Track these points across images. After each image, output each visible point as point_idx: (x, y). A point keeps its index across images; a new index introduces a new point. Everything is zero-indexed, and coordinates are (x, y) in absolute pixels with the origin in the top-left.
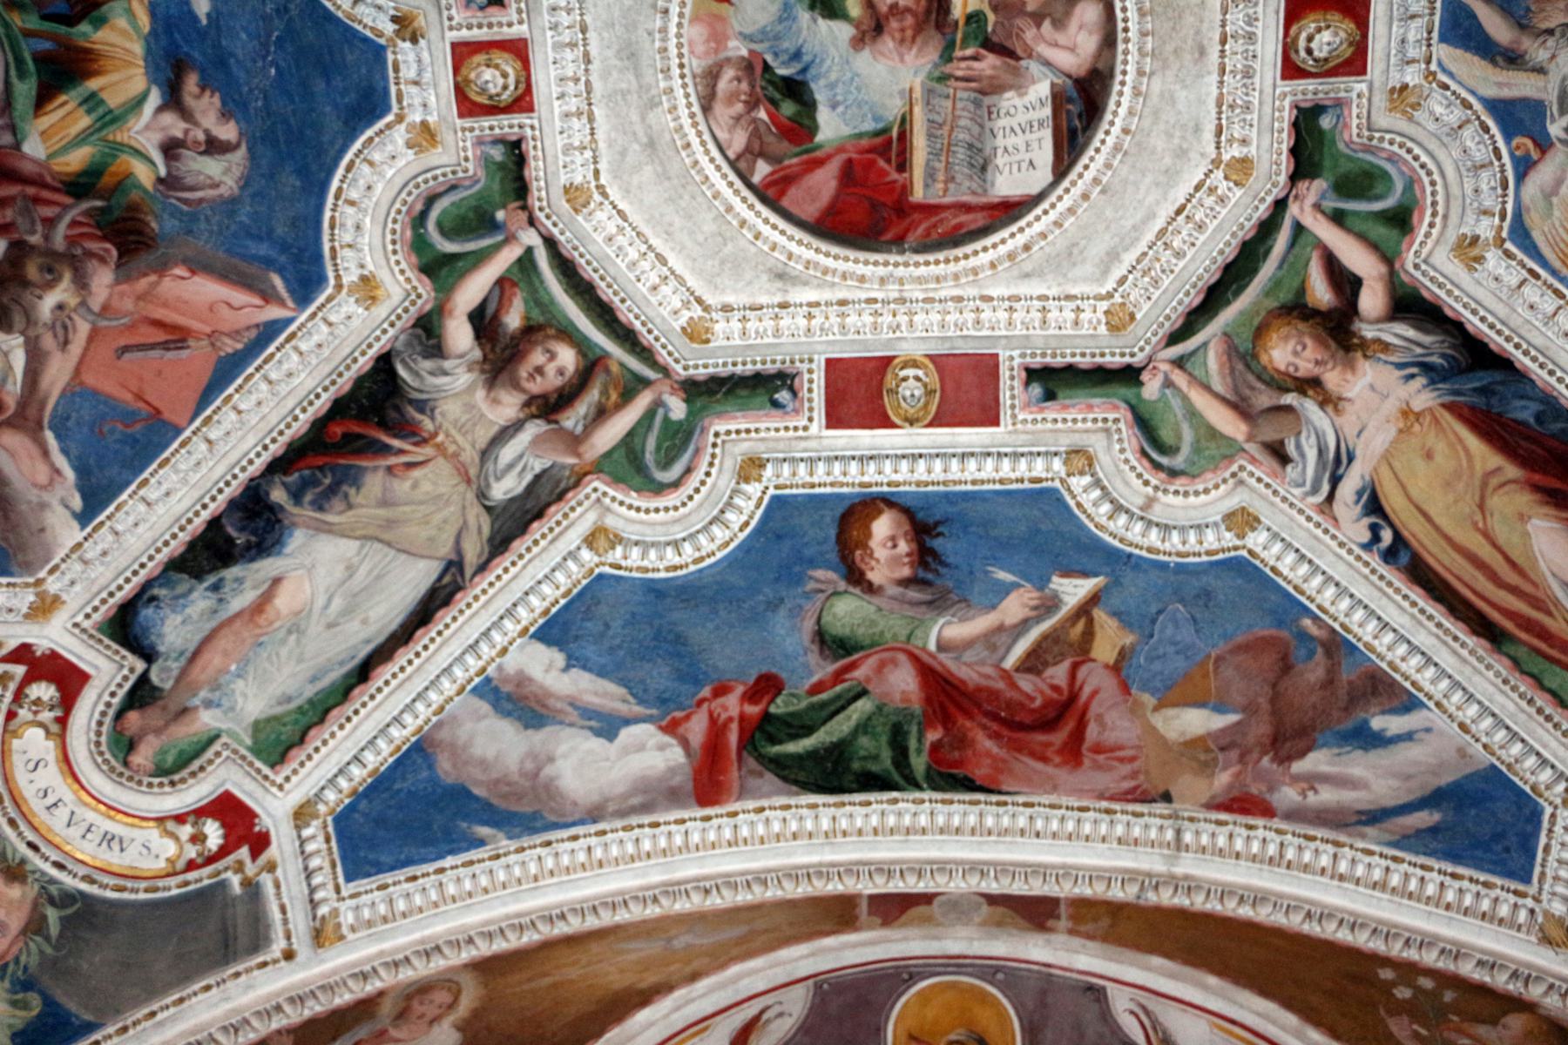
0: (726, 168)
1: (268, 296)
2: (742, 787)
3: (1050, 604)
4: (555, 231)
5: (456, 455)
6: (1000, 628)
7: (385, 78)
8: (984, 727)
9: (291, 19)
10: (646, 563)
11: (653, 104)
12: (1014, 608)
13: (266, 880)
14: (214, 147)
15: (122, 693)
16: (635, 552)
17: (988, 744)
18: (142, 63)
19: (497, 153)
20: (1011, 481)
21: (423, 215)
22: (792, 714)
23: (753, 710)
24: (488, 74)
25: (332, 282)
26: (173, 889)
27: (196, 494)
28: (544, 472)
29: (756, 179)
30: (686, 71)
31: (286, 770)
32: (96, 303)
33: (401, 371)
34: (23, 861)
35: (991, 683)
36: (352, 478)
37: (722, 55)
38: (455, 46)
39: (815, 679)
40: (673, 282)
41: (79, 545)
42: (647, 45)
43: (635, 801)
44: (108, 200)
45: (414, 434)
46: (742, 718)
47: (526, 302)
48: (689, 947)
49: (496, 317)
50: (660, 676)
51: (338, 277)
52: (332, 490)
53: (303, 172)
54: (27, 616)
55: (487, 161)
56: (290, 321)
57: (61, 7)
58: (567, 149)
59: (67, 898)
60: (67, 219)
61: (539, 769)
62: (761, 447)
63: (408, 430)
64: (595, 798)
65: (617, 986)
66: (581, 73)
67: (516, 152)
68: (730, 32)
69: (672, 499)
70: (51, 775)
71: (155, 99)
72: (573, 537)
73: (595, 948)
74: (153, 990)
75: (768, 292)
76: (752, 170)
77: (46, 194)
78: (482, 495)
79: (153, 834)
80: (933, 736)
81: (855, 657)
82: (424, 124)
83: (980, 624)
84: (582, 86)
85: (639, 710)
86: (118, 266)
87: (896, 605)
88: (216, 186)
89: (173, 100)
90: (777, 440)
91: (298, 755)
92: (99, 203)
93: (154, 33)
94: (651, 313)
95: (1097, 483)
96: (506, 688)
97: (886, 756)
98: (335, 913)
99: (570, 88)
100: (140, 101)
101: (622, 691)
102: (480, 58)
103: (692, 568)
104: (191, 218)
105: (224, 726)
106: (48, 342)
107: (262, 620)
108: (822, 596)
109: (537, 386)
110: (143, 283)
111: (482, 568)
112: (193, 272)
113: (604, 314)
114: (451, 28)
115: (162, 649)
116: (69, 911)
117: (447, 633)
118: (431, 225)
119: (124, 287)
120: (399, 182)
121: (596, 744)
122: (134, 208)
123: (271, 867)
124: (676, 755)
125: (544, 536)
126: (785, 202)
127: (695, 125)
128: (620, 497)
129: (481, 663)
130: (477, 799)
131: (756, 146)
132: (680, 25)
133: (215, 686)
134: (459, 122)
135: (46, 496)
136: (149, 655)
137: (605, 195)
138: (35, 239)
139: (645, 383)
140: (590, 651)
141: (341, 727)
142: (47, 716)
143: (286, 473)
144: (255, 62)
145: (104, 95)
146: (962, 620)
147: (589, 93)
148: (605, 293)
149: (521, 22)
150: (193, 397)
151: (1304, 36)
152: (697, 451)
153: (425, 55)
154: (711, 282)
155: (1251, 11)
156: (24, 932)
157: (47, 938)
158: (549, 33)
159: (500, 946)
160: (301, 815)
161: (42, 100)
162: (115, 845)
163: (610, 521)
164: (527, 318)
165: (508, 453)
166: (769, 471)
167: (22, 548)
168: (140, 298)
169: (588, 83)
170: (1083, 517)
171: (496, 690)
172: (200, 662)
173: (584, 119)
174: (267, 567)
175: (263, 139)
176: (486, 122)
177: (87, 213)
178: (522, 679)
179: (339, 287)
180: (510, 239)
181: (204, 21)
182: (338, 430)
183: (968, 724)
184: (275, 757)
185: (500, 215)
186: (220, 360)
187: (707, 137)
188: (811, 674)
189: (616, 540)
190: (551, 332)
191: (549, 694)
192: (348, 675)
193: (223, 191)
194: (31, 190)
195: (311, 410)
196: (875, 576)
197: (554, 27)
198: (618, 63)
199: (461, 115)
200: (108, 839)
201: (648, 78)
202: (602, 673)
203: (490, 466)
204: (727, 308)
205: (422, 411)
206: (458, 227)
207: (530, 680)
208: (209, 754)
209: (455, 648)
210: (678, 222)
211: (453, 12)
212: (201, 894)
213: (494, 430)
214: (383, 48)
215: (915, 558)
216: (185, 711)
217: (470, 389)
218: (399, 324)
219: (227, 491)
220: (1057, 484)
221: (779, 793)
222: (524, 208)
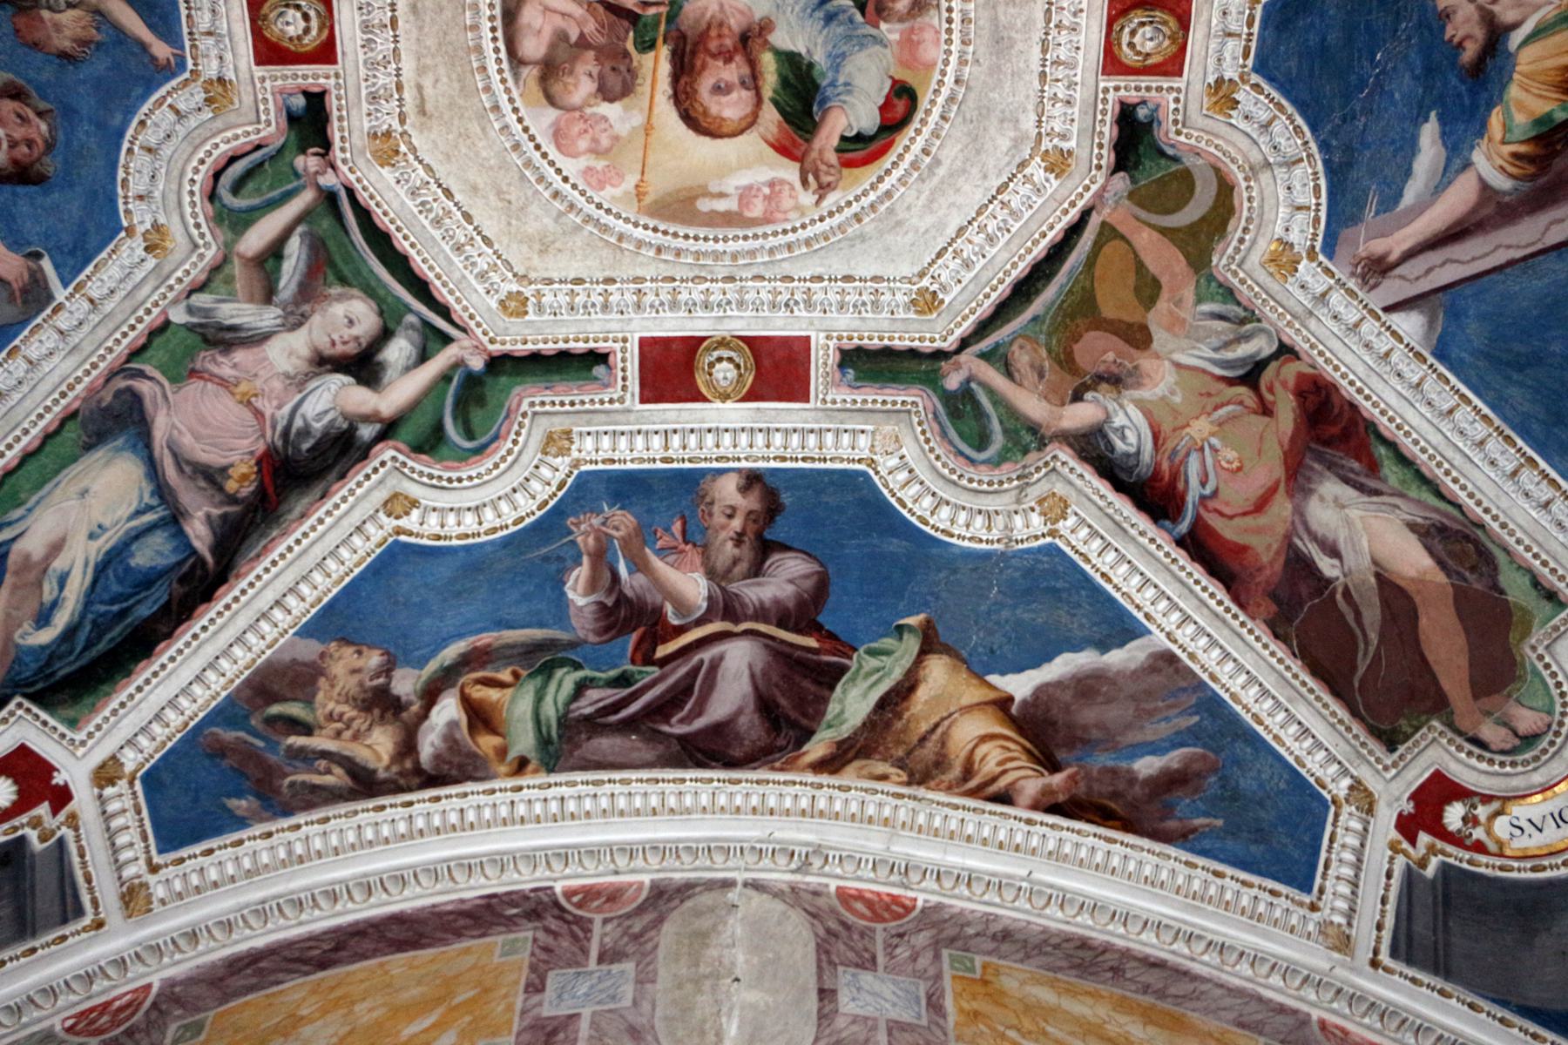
9: (1343, 107)
18: (1516, 76)
24: (1149, 46)
30: (945, 15)
37: (906, 25)
38: (1180, 74)
42: (981, 50)
66: (1054, 32)
68: (895, 47)
71: (1516, 38)
93: (1490, 106)
114: (1179, 90)
132: (946, 62)
144: (1394, 69)
147: (1048, 11)
149: (1106, 90)
151: (314, 32)
155: (370, 54)
158: (1078, 79)
169: (1048, 21)
181: (1433, 114)
198: (1013, 34)
201: (985, 15)
211: (1172, 106)
214: (1256, 70)
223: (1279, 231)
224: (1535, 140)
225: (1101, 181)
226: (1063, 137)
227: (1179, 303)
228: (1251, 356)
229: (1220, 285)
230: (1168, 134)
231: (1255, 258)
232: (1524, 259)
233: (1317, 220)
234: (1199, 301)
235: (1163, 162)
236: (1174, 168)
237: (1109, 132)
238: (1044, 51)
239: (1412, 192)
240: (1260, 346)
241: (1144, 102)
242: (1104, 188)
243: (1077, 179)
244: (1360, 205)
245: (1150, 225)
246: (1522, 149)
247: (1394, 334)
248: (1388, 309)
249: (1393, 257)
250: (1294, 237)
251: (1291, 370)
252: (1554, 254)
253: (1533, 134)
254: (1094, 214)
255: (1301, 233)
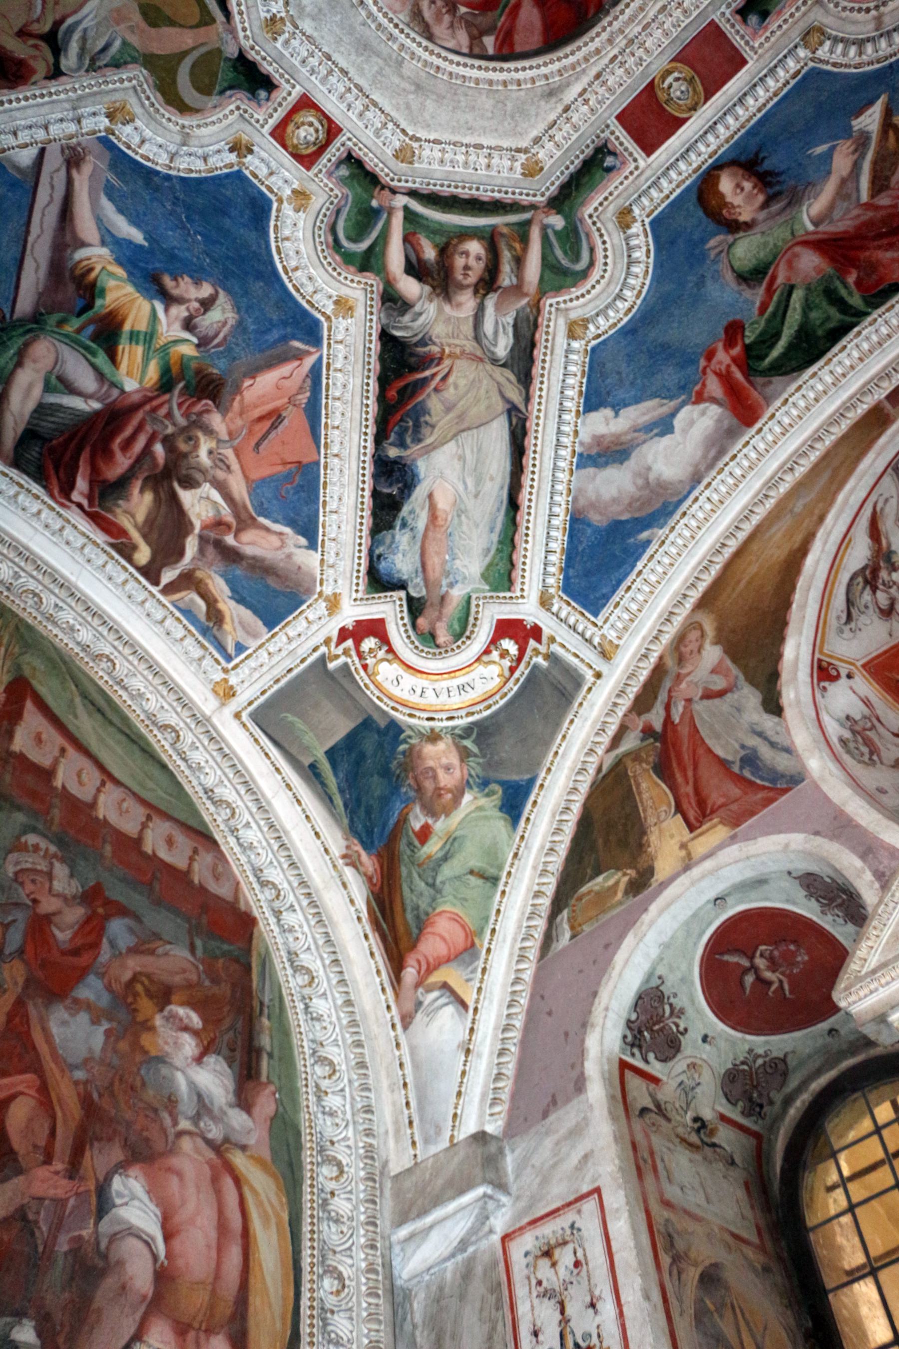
0: (469, 61)
1: (299, 356)
2: (765, 398)
3: (863, 140)
4: (410, 185)
5: (463, 352)
6: (843, 182)
7: (254, 186)
8: (879, 247)
10: (611, 321)
11: (400, 63)
12: (841, 163)
13: (555, 648)
14: (207, 304)
15: (405, 614)
16: (601, 320)
17: (889, 255)
19: (344, 171)
20: (781, 89)
21: (336, 240)
22: (762, 334)
23: (737, 351)
24: (302, 133)
25: (322, 319)
26: (513, 688)
27: (354, 487)
28: (516, 320)
29: (491, 51)
31: (518, 586)
32: (224, 436)
33: (397, 333)
34: (432, 730)
35: (864, 218)
36: (421, 411)
38: (272, 134)
39: (758, 304)
40: (495, 154)
41: (322, 560)
42: (368, 32)
43: (713, 453)
44: (183, 378)
45: (432, 360)
46: (734, 360)
47: (428, 237)
48: (805, 506)
49: (420, 260)
50: (670, 375)
51: (324, 314)
52: (417, 426)
53: (259, 276)
54: (330, 615)
55: (343, 181)
56: (320, 359)
57: (80, 303)
58: (377, 133)
59: (468, 731)
60: (175, 407)
61: (647, 479)
62: (620, 201)
63: (428, 361)
64: (690, 469)
65: (782, 558)
67: (352, 160)
69: (596, 274)
70: (409, 680)
71: (159, 307)
72: (561, 340)
73: (755, 547)
74: (547, 743)
75: (552, 109)
76: (484, 48)
77: (155, 403)
78: (494, 361)
79: (480, 669)
80: (851, 279)
81: (770, 272)
82: (294, 191)
83: (829, 189)
84: (355, 91)
85: (673, 403)
86: (217, 407)
87: (770, 223)
88: (225, 323)
89: (169, 299)
90: (626, 189)
91: (517, 574)
92: (181, 385)
93: (130, 274)
94: (498, 182)
95: (836, 40)
96: (594, 452)
97: (834, 312)
98: (603, 636)
99: (350, 97)
100: (154, 313)
101: (656, 401)
102: (291, 127)
103: (639, 302)
104: (228, 352)
105: (468, 590)
106: (221, 475)
107: (440, 522)
108: (723, 255)
109: (472, 278)
110: (236, 404)
111: (527, 399)
112: (254, 378)
113: (474, 206)
115: (405, 577)
116: (474, 736)
117: (538, 449)
118: (345, 243)
119: (230, 415)
120: (309, 235)
121: (666, 440)
122: (198, 372)
123: (552, 640)
124: (714, 411)
125: (545, 354)
126: (518, 49)
127: (432, 53)
128: (567, 297)
129: (569, 450)
130: (627, 521)
131: (475, 32)
133: (447, 574)
134: (310, 174)
135: (286, 550)
136: (402, 586)
137: (418, 140)
138: (170, 430)
139: (528, 223)
140: (621, 394)
141: (527, 542)
142: (381, 654)
143: (387, 438)
145: (137, 328)
146: (816, 197)
148: (464, 193)
149: (294, 87)
150: (309, 440)
152: (588, 235)
153: (263, 154)
154: (515, 133)
156: (462, 761)
157: (475, 756)
158: (313, 78)
159: (702, 587)
160: (545, 602)
161: (112, 356)
162: (467, 688)
163: (573, 315)
164: (436, 246)
165: (488, 326)
166: (636, 211)
167: (298, 584)
168: (241, 414)
169: (357, 86)
170: (842, 70)
171: (590, 457)
172: (429, 567)
173: (372, 108)
174: (419, 493)
175: (226, 278)
176: (324, 160)
177: (181, 394)
178: (598, 440)
179: (328, 318)
180: (391, 211)
182: (393, 393)
183: (867, 253)
184: (507, 584)
185: (374, 203)
186: (305, 410)
187: (444, 53)
188: (753, 303)
189: (585, 323)
190: (455, 241)
191: (618, 436)
192: (507, 514)
193: (231, 322)
194: (147, 407)
195: (370, 395)
196: (745, 217)
197: (312, 72)
199: (308, 168)
200: (462, 688)
201: (385, 51)
202: (637, 401)
203: (485, 341)
204: (537, 141)
205: (426, 345)
206: (359, 230)
207: (603, 436)
208: (473, 609)
209: (549, 453)
210: (469, 117)
212: (529, 680)
213: (471, 319)
214: (239, 172)
215: (760, 185)
216: (443, 598)
217: (440, 310)
218: (374, 310)
219: (366, 472)
220: (811, 64)
221: (788, 384)
222: (383, 188)
223: (138, 123)
224: (93, 285)
225: (243, 42)
226: (287, 42)
227: (132, 29)
228: (66, 50)
229: (126, 63)
230: (237, 101)
231: (133, 100)
232: (26, 241)
233: (129, 147)
234: (125, 43)
235: (225, 84)
236: (217, 88)
237: (267, 68)
238: (342, 70)
239: (108, 208)
240: (69, 60)
241: (268, 99)
242: (236, 38)
243: (256, 30)
244: (120, 175)
245: (193, 49)
246: (93, 275)
247: (26, 146)
248: (42, 151)
249: (74, 173)
250: (128, 129)
251: (41, 68)
252: (18, 256)
253: (99, 284)
254: (223, 19)
255: (126, 134)
